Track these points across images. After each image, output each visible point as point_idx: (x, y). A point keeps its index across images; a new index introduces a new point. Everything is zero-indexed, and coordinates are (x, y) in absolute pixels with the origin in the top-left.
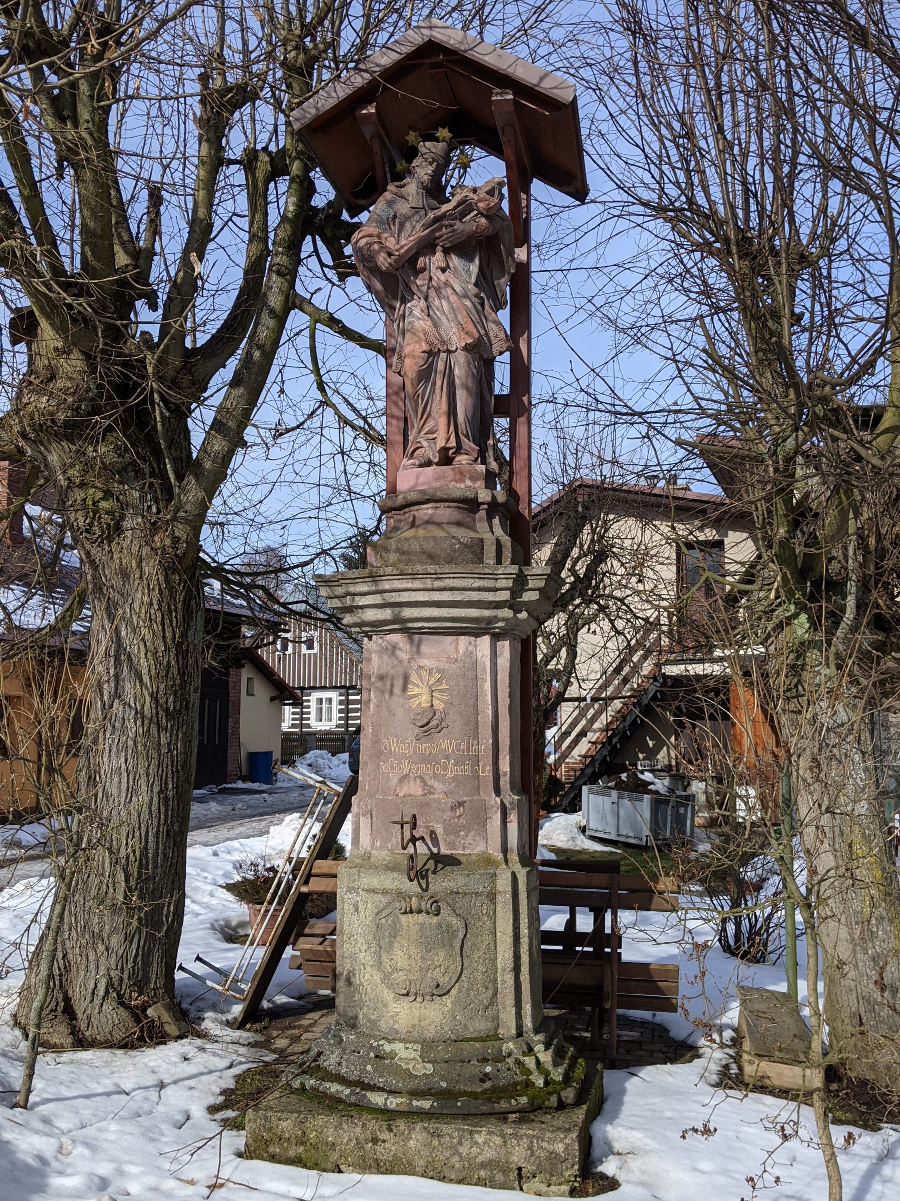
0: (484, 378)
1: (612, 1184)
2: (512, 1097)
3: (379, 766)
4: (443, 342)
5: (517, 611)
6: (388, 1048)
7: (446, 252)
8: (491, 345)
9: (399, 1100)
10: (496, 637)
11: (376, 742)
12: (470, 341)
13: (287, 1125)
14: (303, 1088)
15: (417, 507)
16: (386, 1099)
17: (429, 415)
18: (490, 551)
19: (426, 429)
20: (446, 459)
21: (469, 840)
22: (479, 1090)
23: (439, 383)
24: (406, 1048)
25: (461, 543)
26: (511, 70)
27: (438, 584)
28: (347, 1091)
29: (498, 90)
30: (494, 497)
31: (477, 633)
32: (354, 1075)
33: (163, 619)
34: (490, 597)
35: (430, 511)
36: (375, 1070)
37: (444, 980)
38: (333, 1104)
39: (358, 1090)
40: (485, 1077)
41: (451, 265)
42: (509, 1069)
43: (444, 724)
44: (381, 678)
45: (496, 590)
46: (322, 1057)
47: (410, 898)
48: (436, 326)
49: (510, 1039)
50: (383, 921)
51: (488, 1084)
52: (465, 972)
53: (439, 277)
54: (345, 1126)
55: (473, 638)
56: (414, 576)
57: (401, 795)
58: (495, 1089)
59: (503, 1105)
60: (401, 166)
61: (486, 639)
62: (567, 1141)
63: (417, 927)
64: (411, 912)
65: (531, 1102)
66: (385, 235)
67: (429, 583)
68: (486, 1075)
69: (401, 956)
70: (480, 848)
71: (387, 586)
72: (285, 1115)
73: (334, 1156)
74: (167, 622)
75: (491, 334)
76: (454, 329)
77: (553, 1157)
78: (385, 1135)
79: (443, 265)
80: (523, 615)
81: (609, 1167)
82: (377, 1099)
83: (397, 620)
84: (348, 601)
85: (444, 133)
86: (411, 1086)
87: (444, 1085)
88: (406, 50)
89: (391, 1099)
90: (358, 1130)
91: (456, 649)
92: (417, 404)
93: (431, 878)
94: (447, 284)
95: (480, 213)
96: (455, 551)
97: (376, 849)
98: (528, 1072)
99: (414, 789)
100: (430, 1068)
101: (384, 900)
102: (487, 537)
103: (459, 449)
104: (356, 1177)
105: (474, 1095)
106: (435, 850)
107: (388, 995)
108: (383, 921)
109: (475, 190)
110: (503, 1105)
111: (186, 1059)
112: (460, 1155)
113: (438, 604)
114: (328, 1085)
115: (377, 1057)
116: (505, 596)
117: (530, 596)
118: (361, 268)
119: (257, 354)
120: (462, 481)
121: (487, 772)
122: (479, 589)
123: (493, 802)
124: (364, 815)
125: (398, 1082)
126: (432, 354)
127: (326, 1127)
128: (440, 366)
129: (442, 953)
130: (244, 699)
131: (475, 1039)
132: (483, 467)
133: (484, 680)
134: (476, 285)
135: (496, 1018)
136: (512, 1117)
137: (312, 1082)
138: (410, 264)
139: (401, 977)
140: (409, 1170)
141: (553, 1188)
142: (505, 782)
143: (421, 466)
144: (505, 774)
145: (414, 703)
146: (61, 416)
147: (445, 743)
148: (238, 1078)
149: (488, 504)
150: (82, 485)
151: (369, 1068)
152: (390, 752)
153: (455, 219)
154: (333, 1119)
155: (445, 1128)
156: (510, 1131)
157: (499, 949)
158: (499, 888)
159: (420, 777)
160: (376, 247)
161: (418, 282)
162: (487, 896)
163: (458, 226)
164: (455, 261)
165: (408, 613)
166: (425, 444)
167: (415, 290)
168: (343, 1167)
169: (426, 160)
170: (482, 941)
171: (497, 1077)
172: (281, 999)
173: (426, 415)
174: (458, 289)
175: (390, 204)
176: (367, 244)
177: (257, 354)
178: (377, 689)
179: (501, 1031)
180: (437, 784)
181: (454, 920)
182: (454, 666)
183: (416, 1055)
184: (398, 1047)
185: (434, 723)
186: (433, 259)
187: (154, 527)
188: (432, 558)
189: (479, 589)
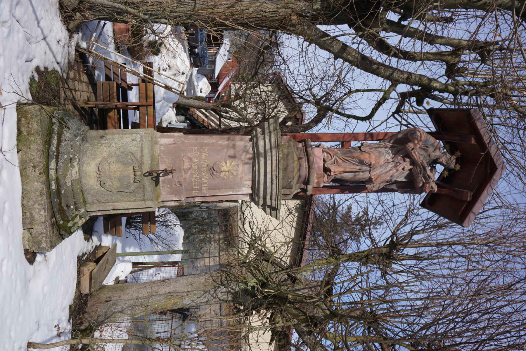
3: (195, 146)
4: (374, 169)
6: (75, 164)
7: (410, 170)
9: (53, 175)
10: (251, 195)
11: (206, 145)
12: (373, 180)
13: (35, 126)
14: (53, 124)
15: (306, 160)
16: (53, 169)
19: (339, 160)
20: (326, 170)
21: (166, 189)
22: (63, 205)
24: (76, 173)
25: (291, 182)
26: (479, 201)
27: (274, 178)
28: (54, 149)
31: (253, 188)
32: (62, 150)
33: (258, 17)
34: (268, 197)
35: (305, 166)
36: (65, 160)
37: (107, 185)
38: (48, 143)
39: (55, 154)
40: (68, 206)
45: (271, 199)
46: (67, 129)
50: (129, 157)
51: (65, 208)
54: (39, 153)
58: (64, 211)
59: (58, 216)
61: (250, 192)
62: (47, 248)
63: (128, 174)
67: (274, 173)
68: (70, 206)
70: (163, 193)
72: (39, 125)
73: (24, 149)
74: (257, 19)
78: (37, 172)
82: (53, 165)
84: (267, 131)
86: (60, 178)
87: (63, 192)
88: (495, 159)
89: (53, 171)
90: (38, 159)
91: (246, 180)
92: (349, 157)
93: (149, 178)
95: (424, 184)
96: (288, 180)
97: (160, 147)
98: (73, 219)
99: (186, 165)
100: (70, 184)
102: (293, 189)
103: (328, 175)
104: (16, 162)
105: (60, 204)
106: (161, 175)
107: (98, 161)
108: (129, 157)
110: (58, 216)
111: (58, 42)
112: (34, 205)
114: (56, 138)
115: (71, 159)
116: (268, 202)
119: (375, 67)
123: (182, 197)
124: (174, 140)
125: (61, 172)
128: (364, 168)
129: (118, 185)
131: (84, 198)
133: (233, 191)
136: (54, 219)
137: (56, 129)
138: (407, 155)
139: (107, 167)
140: (24, 183)
141: (27, 243)
142: (191, 200)
144: (194, 200)
145: (223, 164)
147: (206, 178)
148: (54, 70)
151: (66, 156)
152: (201, 152)
154: (41, 147)
155: (44, 198)
156: (47, 224)
158: (147, 202)
159: (191, 167)
160: (416, 142)
164: (406, 173)
165: (262, 160)
166: (333, 160)
167: (397, 156)
168: (20, 153)
169: (448, 160)
171: (69, 210)
175: (433, 145)
177: (375, 67)
178: (228, 144)
179: (88, 205)
180: (188, 175)
181: (132, 188)
182: (239, 180)
183: (74, 177)
184: (76, 168)
185: (215, 173)
186: (408, 164)
187: (300, 15)
188: (286, 169)
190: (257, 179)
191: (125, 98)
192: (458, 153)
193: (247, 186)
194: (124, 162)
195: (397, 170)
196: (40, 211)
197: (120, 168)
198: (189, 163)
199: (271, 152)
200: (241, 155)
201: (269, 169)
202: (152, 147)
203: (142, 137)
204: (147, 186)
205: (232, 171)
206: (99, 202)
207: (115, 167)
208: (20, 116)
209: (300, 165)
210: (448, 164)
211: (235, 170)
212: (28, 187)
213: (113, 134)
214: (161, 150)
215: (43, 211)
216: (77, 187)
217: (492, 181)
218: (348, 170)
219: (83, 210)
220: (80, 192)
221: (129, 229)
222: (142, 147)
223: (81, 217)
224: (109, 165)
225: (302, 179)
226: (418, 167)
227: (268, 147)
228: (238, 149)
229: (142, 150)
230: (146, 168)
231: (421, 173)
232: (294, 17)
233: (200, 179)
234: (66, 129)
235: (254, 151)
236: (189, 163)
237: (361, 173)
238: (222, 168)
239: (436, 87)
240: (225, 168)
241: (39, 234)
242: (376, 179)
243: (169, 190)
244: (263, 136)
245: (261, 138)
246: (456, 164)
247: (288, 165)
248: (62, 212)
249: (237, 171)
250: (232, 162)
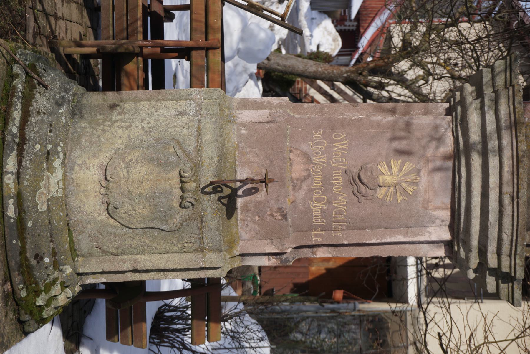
2: (25, 284)
3: (319, 127)
5: (475, 271)
6: (57, 163)
9: (12, 186)
10: (449, 245)
11: (344, 124)
14: (13, 77)
16: (12, 173)
21: (251, 225)
22: (28, 255)
24: (58, 183)
27: (507, 200)
28: (15, 130)
31: (453, 227)
32: (30, 134)
34: (492, 248)
36: (36, 154)
37: (122, 213)
39: (17, 140)
40: (39, 258)
42: (48, 275)
43: (362, 199)
44: (408, 125)
45: (499, 253)
46: (42, 90)
47: (194, 181)
49: (74, 268)
51: (33, 262)
52: (131, 231)
55: (448, 223)
56: (516, 172)
57: (292, 156)
58: (30, 268)
61: (447, 236)
63: (168, 188)
64: (182, 182)
65: (21, 299)
67: (507, 189)
68: (42, 258)
69: (140, 174)
70: (244, 234)
71: (506, 141)
80: (471, 275)
83: (468, 148)
84: (488, 92)
86: (26, 194)
87: (30, 225)
91: (438, 208)
97: (239, 130)
98: (47, 289)
99: (298, 170)
100: (43, 208)
101: (191, 149)
105: (23, 251)
106: (240, 192)
107: (104, 158)
108: (172, 150)
110: (17, 279)
114: (19, 107)
115: (48, 153)
116: (492, 262)
123: (287, 245)
124: (270, 114)
125: (28, 180)
129: (146, 212)
131: (72, 241)
135: (91, 255)
136: (8, 286)
137: (20, 87)
142: (306, 253)
144: (314, 253)
145: (383, 168)
147: (343, 201)
151: (38, 147)
152: (333, 141)
157: (153, 256)
158: (208, 256)
159: (309, 175)
162: (200, 246)
170: (159, 244)
178: (395, 122)
179: (80, 259)
181: (176, 220)
183: (53, 194)
184: (59, 174)
185: (363, 189)
190: (463, 204)
191: (158, 33)
193: (438, 222)
194: (159, 160)
197: (150, 174)
198: (303, 167)
199: (500, 138)
200: (425, 148)
201: (493, 180)
202: (221, 128)
203: (199, 106)
204: (209, 217)
205: (404, 185)
206: (104, 252)
207: (140, 171)
211: (411, 183)
213: (136, 100)
214: (240, 136)
219: (68, 270)
221: (158, 345)
222: (199, 128)
223: (64, 286)
224: (128, 168)
227: (491, 127)
228: (418, 134)
229: (199, 135)
230: (208, 176)
233: (329, 202)
236: (303, 167)
238: (381, 177)
240: (387, 178)
243: (256, 226)
244: (479, 101)
245: (474, 105)
248: (26, 270)
249: (416, 184)
250: (403, 164)
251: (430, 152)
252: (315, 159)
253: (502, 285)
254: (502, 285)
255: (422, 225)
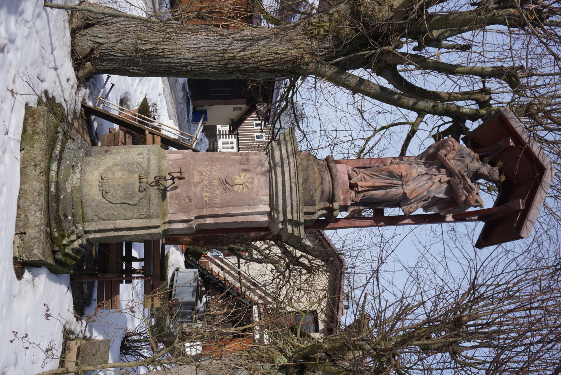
0: (391, 203)
1: (19, 276)
2: (57, 229)
3: (206, 161)
4: (407, 182)
6: (78, 170)
7: (448, 182)
8: (407, 205)
9: (54, 176)
10: (269, 214)
12: (408, 195)
13: (41, 125)
14: (57, 133)
15: (329, 173)
16: (54, 170)
17: (372, 177)
18: (311, 209)
19: (366, 177)
20: (353, 186)
21: (174, 205)
22: (60, 214)
23: (388, 181)
25: (313, 194)
26: (534, 207)
28: (57, 153)
29: (524, 202)
30: (336, 210)
31: (271, 205)
32: (65, 156)
33: (270, 60)
35: (327, 180)
36: (67, 165)
37: (109, 196)
38: (51, 147)
40: (66, 216)
41: (442, 185)
42: (70, 227)
43: (227, 191)
44: (248, 160)
45: (292, 212)
46: (72, 141)
47: (146, 178)
48: (414, 179)
49: (83, 227)
50: (135, 166)
51: (63, 218)
52: (113, 205)
53: (437, 179)
54: (41, 152)
55: (268, 203)
56: (297, 172)
57: (193, 172)
59: (54, 225)
60: (487, 159)
61: (268, 209)
62: (39, 255)
63: (133, 182)
64: (140, 179)
65: (55, 238)
66: (455, 153)
67: (293, 180)
68: (67, 217)
70: (170, 210)
71: (291, 160)
72: (45, 124)
73: (27, 147)
74: (269, 62)
75: (411, 205)
76: (413, 187)
77: (31, 248)
78: (38, 170)
79: (442, 181)
80: (280, 226)
81: (27, 275)
82: (54, 166)
84: (283, 142)
85: (503, 178)
87: (62, 197)
88: (540, 158)
89: (55, 173)
90: (40, 158)
91: (263, 195)
92: (377, 171)
93: (156, 188)
94: (434, 183)
95: (467, 197)
96: (309, 192)
97: (168, 162)
98: (69, 237)
99: (196, 178)
100: (69, 190)
101: (145, 166)
102: (317, 207)
103: (358, 192)
104: (19, 157)
105: (57, 211)
106: (168, 189)
107: (101, 170)
109: (477, 194)
110: (54, 225)
111: (68, 80)
112: (30, 205)
113: (284, 185)
114: (60, 144)
115: (73, 166)
116: (289, 217)
117: (290, 229)
118: (438, 143)
119: (396, 97)
120: (343, 194)
121: (206, 212)
122: (292, 204)
124: (183, 155)
126: (401, 177)
127: (41, 143)
128: (395, 182)
129: (122, 194)
130: (231, 107)
131: (83, 211)
132: (349, 204)
133: (249, 209)
134: (434, 197)
135: (93, 221)
136: (48, 229)
137: (61, 137)
138: (442, 165)
139: (110, 175)
140: (23, 182)
141: (17, 249)
142: (201, 221)
143: (349, 175)
144: (205, 221)
146: (362, 9)
147: (218, 191)
148: (60, 105)
149: (332, 207)
150: (330, 20)
151: (68, 162)
152: (213, 166)
153: (464, 185)
154: (44, 146)
155: (42, 198)
156: (42, 228)
157: (125, 221)
158: (153, 220)
161: (434, 170)
162: (149, 214)
163: (461, 186)
164: (445, 186)
165: (279, 170)
166: (359, 176)
167: (431, 168)
168: (23, 151)
169: (490, 170)
170: (128, 213)
171: (66, 222)
172: (95, 124)
173: (372, 176)
174: (432, 188)
175: (469, 155)
176: (450, 144)
178: (242, 158)
179: (87, 223)
180: (199, 189)
183: (75, 184)
184: (78, 175)
186: (445, 176)
187: (312, 54)
188: (306, 180)
189: (292, 204)
190: (274, 191)
192: (500, 163)
193: (264, 202)
194: (129, 170)
195: (434, 183)
196: (36, 213)
197: (124, 175)
198: (199, 177)
199: (288, 159)
200: (256, 168)
201: (287, 177)
202: (159, 160)
204: (153, 198)
205: (247, 184)
208: (27, 116)
209: (322, 179)
210: (490, 174)
211: (250, 183)
212: (26, 187)
215: (39, 212)
216: (77, 195)
217: (543, 184)
218: (377, 184)
220: (78, 199)
221: (125, 354)
222: (149, 159)
224: (113, 173)
225: (326, 195)
226: (456, 177)
228: (252, 163)
229: (149, 161)
231: (460, 184)
232: (307, 58)
234: (70, 140)
235: (270, 164)
236: (199, 177)
237: (393, 189)
238: (236, 181)
239: (466, 112)
240: (238, 181)
241: (33, 239)
242: (411, 193)
243: (177, 206)
245: (277, 149)
246: (500, 175)
247: (308, 176)
248: (59, 222)
250: (246, 175)
251: (258, 170)
252: (204, 174)
253: (295, 229)
254: (295, 229)
255: (256, 204)
